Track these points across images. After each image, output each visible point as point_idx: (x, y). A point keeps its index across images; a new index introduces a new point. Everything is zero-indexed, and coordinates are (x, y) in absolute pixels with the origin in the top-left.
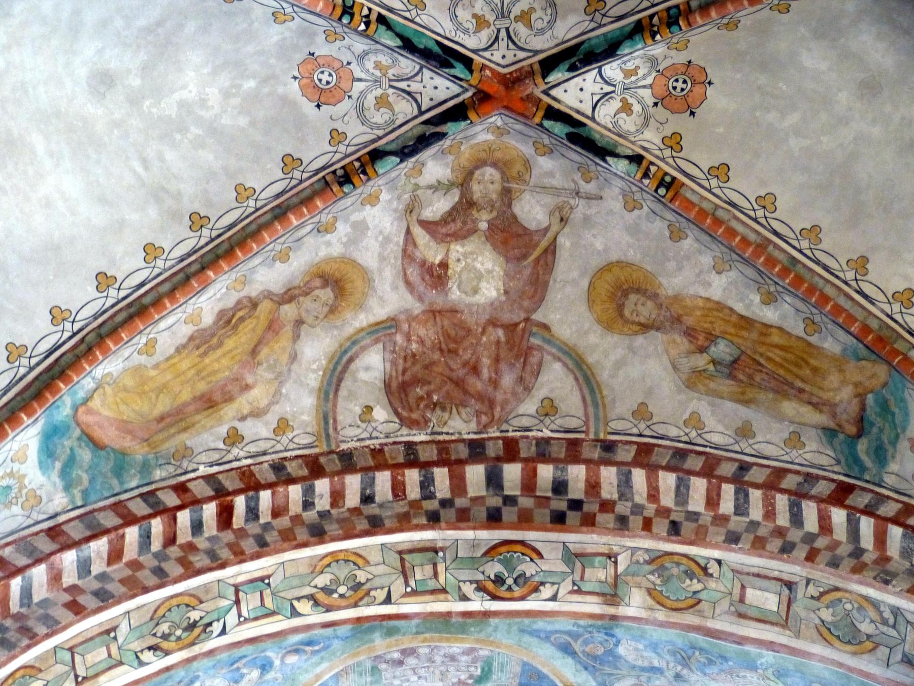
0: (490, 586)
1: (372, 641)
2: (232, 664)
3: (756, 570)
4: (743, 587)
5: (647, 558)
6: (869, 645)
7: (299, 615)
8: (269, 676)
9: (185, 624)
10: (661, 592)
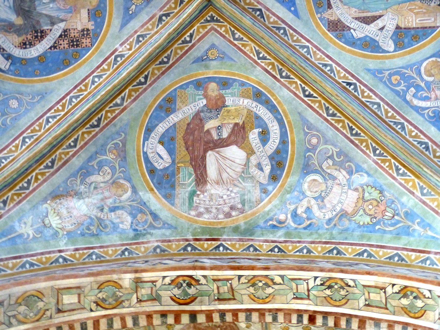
0: (193, 282)
1: (245, 223)
2: (310, 225)
3: (75, 312)
4: (79, 302)
5: (124, 304)
6: (19, 301)
7: (280, 276)
8: (292, 207)
9: (333, 289)
10: (116, 288)
